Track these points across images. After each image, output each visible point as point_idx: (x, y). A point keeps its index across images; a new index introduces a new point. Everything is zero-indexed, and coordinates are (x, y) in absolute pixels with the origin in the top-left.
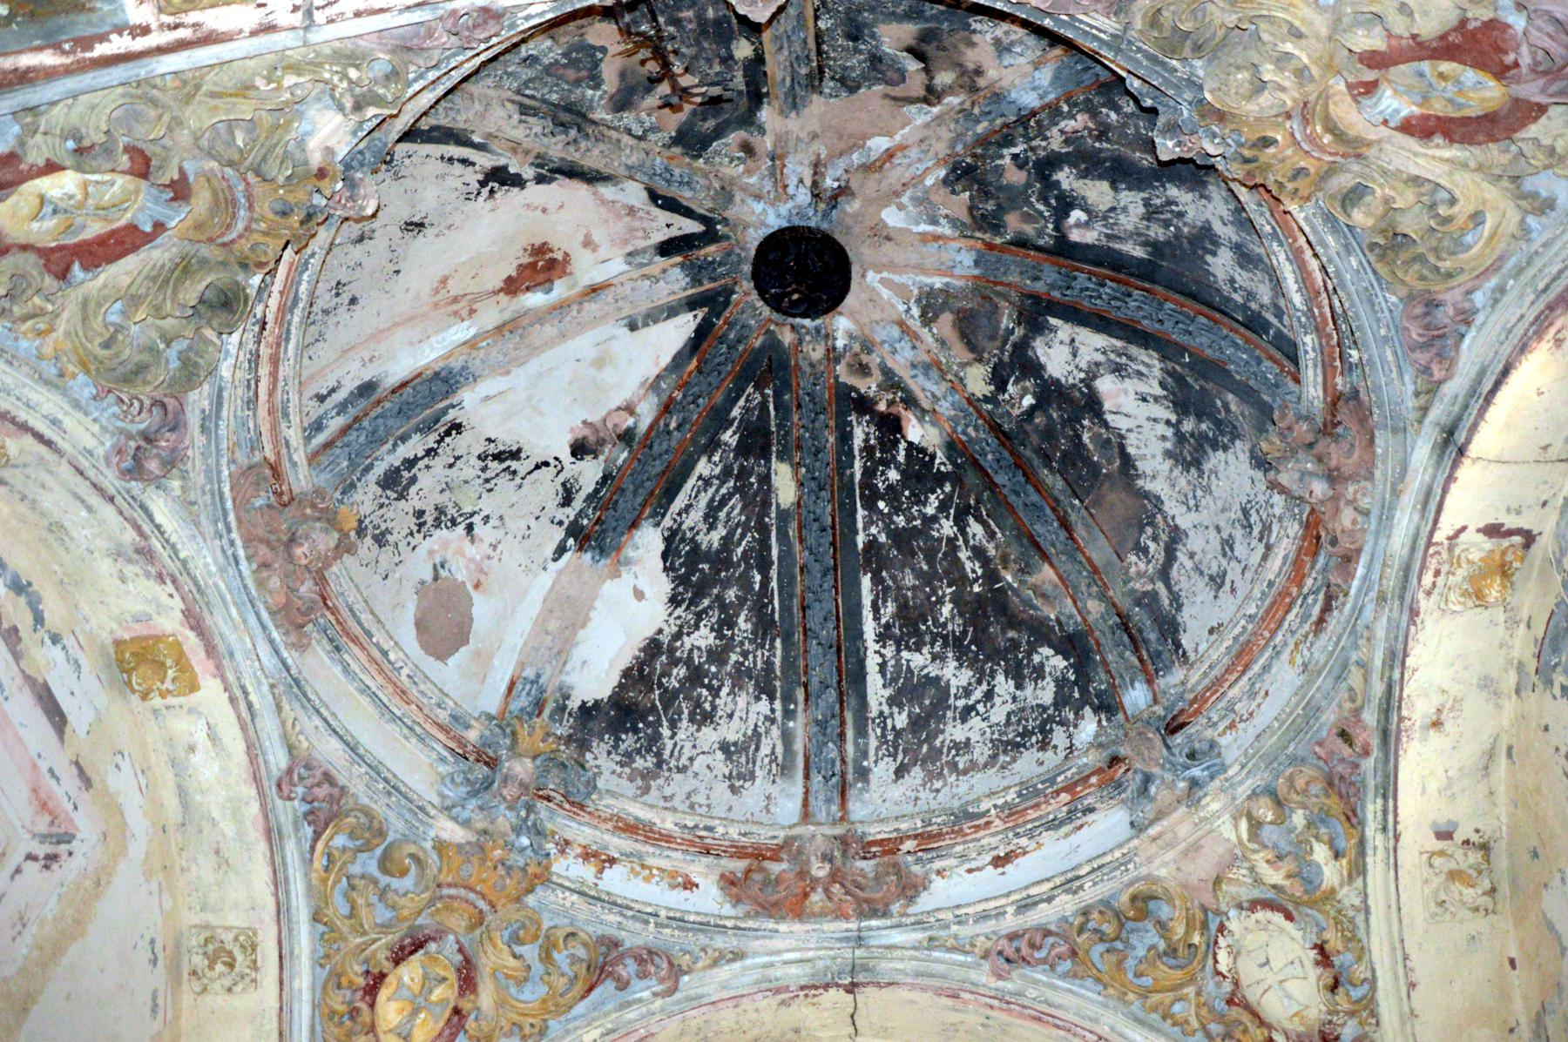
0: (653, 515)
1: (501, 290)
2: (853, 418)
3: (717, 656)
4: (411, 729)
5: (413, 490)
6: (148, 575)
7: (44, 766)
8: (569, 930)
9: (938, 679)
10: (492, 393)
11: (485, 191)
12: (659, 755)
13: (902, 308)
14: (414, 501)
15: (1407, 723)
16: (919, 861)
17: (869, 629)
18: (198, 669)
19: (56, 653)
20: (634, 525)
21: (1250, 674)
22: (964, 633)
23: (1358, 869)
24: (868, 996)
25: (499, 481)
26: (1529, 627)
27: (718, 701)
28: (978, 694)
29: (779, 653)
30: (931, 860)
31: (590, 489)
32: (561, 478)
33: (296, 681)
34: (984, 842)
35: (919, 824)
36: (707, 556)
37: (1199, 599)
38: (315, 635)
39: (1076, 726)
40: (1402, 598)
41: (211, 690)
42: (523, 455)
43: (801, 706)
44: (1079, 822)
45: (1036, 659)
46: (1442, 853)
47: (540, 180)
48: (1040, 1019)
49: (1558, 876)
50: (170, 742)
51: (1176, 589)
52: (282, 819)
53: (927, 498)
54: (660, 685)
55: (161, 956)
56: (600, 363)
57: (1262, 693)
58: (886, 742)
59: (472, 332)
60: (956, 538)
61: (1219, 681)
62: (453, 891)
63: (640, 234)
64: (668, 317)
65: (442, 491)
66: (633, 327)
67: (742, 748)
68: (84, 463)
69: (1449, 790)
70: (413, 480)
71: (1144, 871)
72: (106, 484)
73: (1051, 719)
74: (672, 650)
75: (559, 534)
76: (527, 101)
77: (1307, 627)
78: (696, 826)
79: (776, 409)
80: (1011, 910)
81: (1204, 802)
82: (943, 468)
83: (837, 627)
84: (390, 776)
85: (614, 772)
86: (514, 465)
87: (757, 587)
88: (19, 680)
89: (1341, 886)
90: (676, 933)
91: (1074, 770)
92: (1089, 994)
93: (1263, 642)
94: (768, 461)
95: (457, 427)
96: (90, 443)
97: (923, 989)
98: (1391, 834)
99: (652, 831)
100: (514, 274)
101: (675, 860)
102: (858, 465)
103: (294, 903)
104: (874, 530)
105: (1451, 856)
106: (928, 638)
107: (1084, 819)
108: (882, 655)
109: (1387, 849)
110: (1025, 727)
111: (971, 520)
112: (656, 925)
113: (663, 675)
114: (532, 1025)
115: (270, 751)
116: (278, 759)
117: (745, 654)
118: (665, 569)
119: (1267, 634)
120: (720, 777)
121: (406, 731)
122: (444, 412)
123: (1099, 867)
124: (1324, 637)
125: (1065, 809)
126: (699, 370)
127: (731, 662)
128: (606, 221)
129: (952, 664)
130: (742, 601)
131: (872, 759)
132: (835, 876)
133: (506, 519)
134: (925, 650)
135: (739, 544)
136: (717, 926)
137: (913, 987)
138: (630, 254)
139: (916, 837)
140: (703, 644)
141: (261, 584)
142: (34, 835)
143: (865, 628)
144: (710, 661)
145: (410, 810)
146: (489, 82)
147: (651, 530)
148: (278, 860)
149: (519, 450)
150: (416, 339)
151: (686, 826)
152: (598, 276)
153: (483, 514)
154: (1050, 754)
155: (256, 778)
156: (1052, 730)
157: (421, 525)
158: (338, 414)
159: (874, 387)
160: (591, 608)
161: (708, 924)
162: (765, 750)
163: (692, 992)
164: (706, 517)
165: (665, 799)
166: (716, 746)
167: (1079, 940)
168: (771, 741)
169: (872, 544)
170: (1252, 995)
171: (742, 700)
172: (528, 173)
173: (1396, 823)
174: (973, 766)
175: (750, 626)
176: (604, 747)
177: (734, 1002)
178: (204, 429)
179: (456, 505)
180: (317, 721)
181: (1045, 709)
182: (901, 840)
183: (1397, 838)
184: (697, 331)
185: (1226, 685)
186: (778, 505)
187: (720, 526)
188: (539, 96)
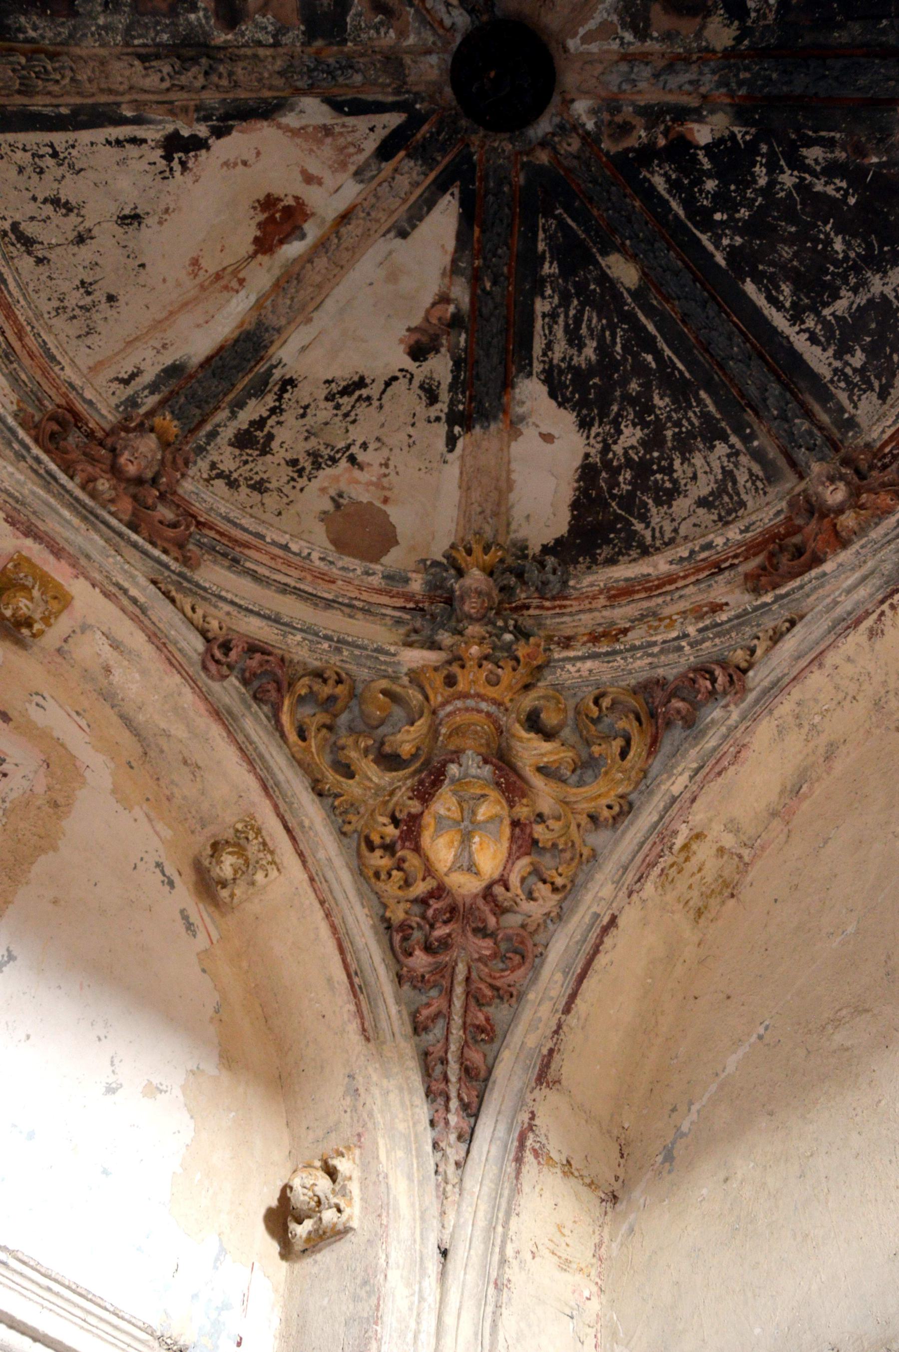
0: (521, 369)
1: (256, 253)
2: (644, 173)
3: (653, 441)
5: (275, 445)
8: (597, 692)
9: (870, 301)
10: (305, 342)
11: (175, 164)
13: (615, 46)
14: (280, 454)
17: (779, 321)
18: (59, 579)
20: (507, 384)
22: (869, 247)
25: (358, 411)
27: (675, 475)
29: (708, 401)
31: (449, 380)
32: (416, 383)
36: (592, 371)
38: (206, 557)
42: (368, 381)
47: (220, 132)
52: (227, 700)
53: (753, 174)
54: (613, 497)
56: (393, 277)
58: (856, 385)
59: (253, 298)
60: (802, 179)
63: (352, 150)
64: (429, 210)
65: (306, 439)
66: (403, 234)
67: (718, 493)
70: (270, 437)
74: (607, 464)
75: (442, 429)
76: (142, 51)
78: (692, 552)
79: (574, 220)
82: (748, 138)
83: (747, 340)
84: (330, 633)
86: (364, 392)
87: (654, 365)
90: (717, 641)
94: (597, 264)
95: (289, 383)
100: (258, 233)
102: (674, 204)
103: (281, 777)
104: (725, 242)
108: (807, 330)
111: (804, 151)
112: (691, 645)
113: (611, 488)
114: (610, 807)
115: (179, 638)
117: (678, 424)
118: (560, 405)
122: (269, 373)
126: (483, 232)
128: (311, 150)
130: (647, 387)
133: (385, 439)
134: (843, 293)
135: (614, 343)
136: (756, 609)
138: (356, 174)
140: (633, 441)
141: (93, 495)
143: (775, 323)
144: (649, 450)
145: (368, 657)
146: (90, 41)
147: (527, 381)
148: (241, 738)
149: (362, 378)
150: (201, 321)
151: (682, 559)
152: (340, 204)
153: (358, 444)
155: (179, 669)
157: (300, 472)
158: (152, 393)
159: (643, 133)
160: (509, 472)
161: (745, 613)
162: (742, 478)
163: (766, 683)
164: (570, 342)
169: (732, 254)
171: (698, 460)
172: (202, 130)
175: (667, 400)
177: (816, 663)
179: (327, 445)
180: (227, 608)
184: (462, 204)
186: (628, 290)
187: (587, 342)
188: (150, 42)
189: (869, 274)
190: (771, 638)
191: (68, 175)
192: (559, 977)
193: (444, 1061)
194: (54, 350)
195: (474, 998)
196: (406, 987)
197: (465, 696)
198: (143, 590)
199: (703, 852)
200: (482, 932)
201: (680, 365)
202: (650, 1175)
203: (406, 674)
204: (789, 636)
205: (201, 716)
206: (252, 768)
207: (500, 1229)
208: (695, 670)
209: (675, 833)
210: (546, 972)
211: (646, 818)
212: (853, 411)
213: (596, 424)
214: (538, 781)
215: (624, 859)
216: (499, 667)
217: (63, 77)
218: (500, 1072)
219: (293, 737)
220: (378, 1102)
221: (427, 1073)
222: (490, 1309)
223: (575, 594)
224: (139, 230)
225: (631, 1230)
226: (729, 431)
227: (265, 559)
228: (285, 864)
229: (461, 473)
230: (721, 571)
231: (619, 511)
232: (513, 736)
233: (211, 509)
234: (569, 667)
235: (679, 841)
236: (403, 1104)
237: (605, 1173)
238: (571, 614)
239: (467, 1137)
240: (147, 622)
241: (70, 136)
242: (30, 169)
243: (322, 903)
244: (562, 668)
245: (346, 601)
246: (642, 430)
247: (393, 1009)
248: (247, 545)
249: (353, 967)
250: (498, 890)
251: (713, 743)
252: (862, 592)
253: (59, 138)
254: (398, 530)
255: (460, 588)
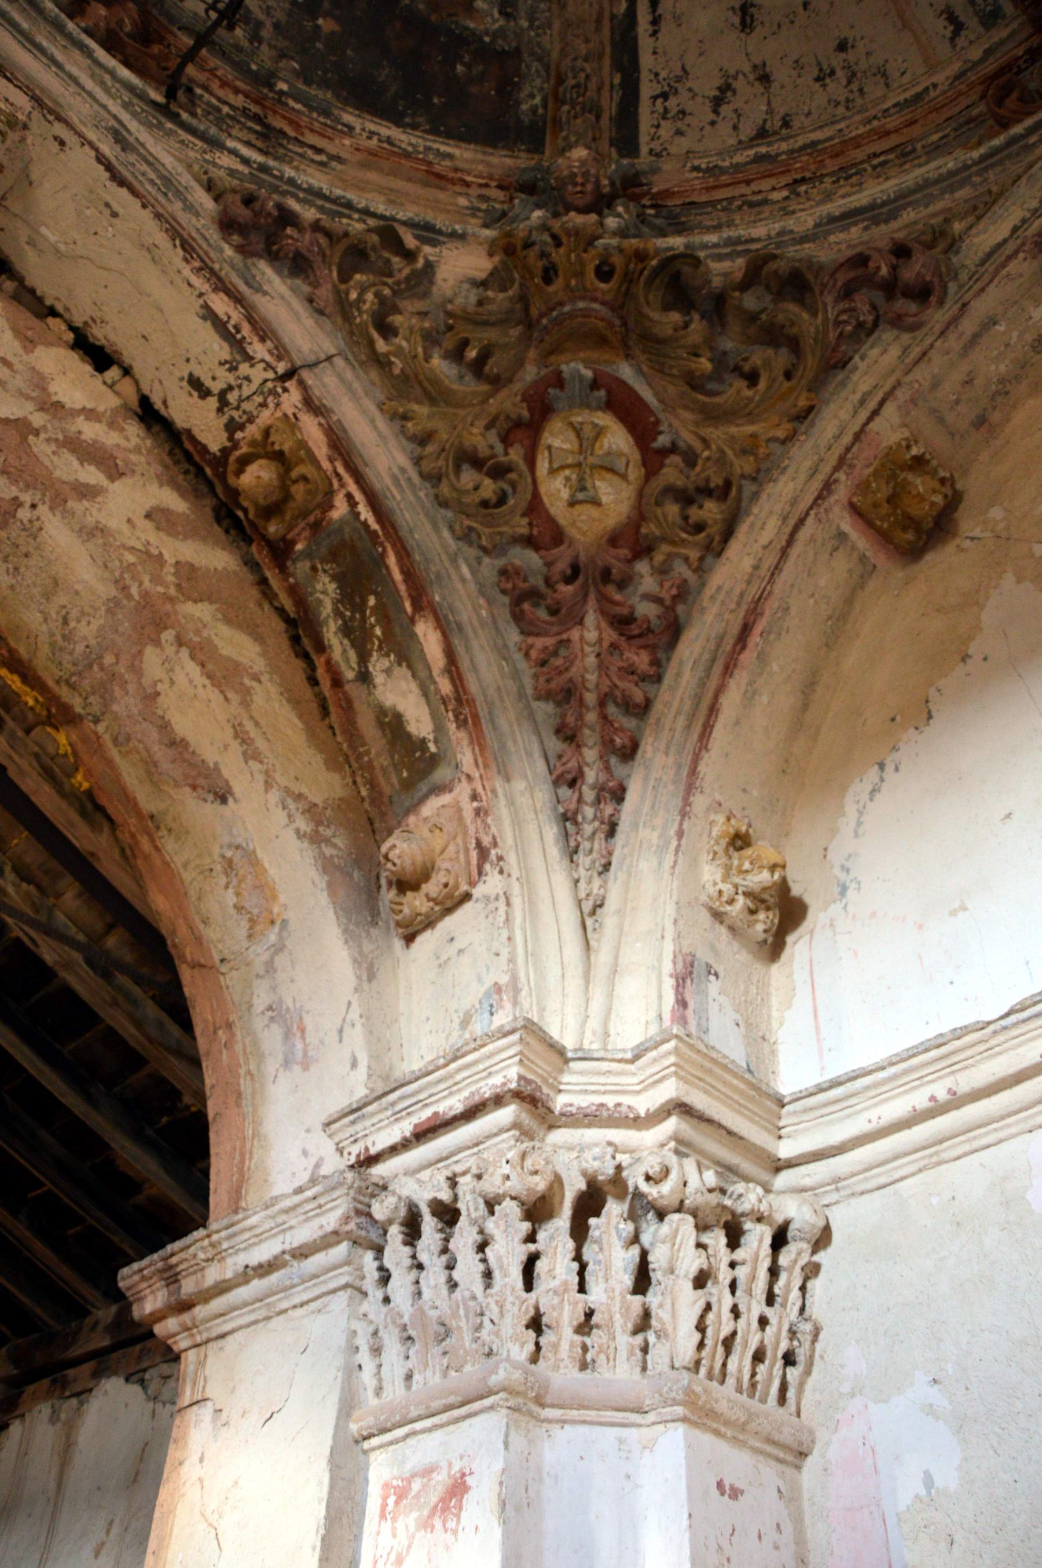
68: (916, 352)
72: (947, 317)
96: (895, 352)
178: (893, 215)
191: (689, 85)
194: (907, 95)
217: (583, 70)
224: (760, 7)
241: (645, 76)
242: (679, 124)
253: (647, 89)
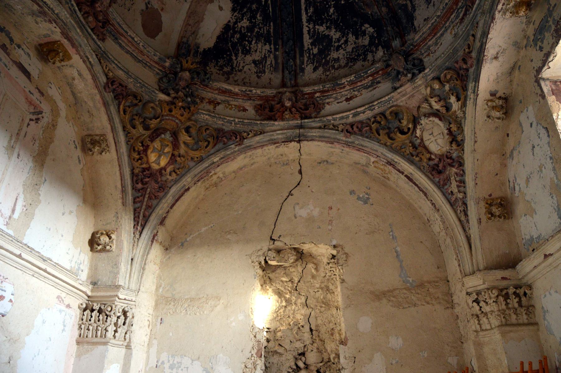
3: (250, 29)
4: (146, 64)
6: (45, 21)
7: (27, 90)
8: (206, 127)
9: (329, 35)
12: (232, 66)
15: (486, 57)
16: (321, 99)
17: (304, 18)
19: (20, 51)
21: (436, 37)
22: (338, 19)
23: (464, 105)
24: (304, 144)
26: (534, 24)
27: (251, 46)
28: (342, 41)
29: (272, 27)
30: (325, 99)
33: (104, 52)
34: (343, 93)
35: (321, 87)
37: (421, 8)
39: (376, 53)
40: (490, 13)
41: (76, 59)
43: (280, 47)
44: (375, 87)
45: (363, 28)
46: (491, 101)
48: (359, 150)
49: (526, 109)
50: (65, 77)
51: (414, 3)
52: (108, 99)
54: (231, 41)
55: (78, 146)
57: (440, 44)
58: (310, 59)
61: (425, 39)
62: (167, 118)
69: (497, 80)
71: (395, 103)
73: (367, 50)
74: (234, 28)
77: (458, 20)
78: (246, 90)
80: (351, 116)
81: (416, 81)
84: (141, 82)
85: (217, 73)
88: (11, 63)
89: (458, 110)
90: (241, 126)
91: (374, 69)
92: (375, 143)
93: (441, 25)
97: (322, 141)
98: (476, 94)
99: (231, 93)
101: (240, 102)
103: (116, 125)
105: (494, 101)
106: (325, 21)
107: (377, 86)
108: (309, 27)
109: (474, 99)
110: (358, 53)
113: (231, 38)
114: (197, 158)
116: (103, 79)
117: (260, 28)
119: (443, 23)
120: (253, 73)
121: (144, 65)
123: (380, 102)
124: (463, 24)
125: (370, 82)
127: (255, 31)
129: (334, 30)
131: (306, 65)
132: (293, 106)
134: (324, 25)
137: (319, 141)
139: (320, 92)
140: (245, 25)
142: (30, 113)
144: (248, 32)
148: (109, 113)
151: (242, 91)
154: (366, 63)
155: (97, 87)
156: (367, 54)
160: (204, 15)
162: (268, 63)
163: (248, 144)
165: (235, 81)
166: (251, 62)
167: (373, 126)
168: (270, 60)
170: (427, 143)
171: (260, 45)
173: (478, 90)
174: (340, 67)
175: (261, 18)
176: (213, 64)
180: (114, 66)
181: (365, 46)
182: (315, 93)
183: (477, 95)
185: (428, 40)
189: (333, 27)
190: (254, 134)
192: (171, 198)
193: (139, 213)
195: (150, 198)
196: (134, 190)
197: (173, 116)
198: (94, 59)
199: (215, 177)
200: (157, 182)
201: (270, 9)
202: (177, 247)
203: (158, 101)
204: (258, 136)
205: (100, 104)
206: (110, 124)
207: (145, 256)
208: (233, 133)
209: (211, 172)
210: (168, 196)
211: (205, 164)
212: (306, 67)
213: (237, 12)
214: (182, 146)
215: (196, 173)
216: (185, 111)
218: (152, 218)
219: (122, 113)
220: (124, 221)
221: (134, 214)
222: (141, 274)
223: (210, 86)
225: (169, 258)
226: (272, 43)
227: (126, 41)
228: (112, 151)
229: (189, 8)
230: (250, 99)
231: (230, 48)
232: (181, 132)
233: (115, 19)
234: (202, 115)
235: (211, 174)
236: (128, 222)
237: (167, 244)
238: (206, 91)
239: (141, 233)
240: (92, 71)
243: (119, 166)
244: (200, 115)
245: (145, 62)
246: (249, 23)
247: (130, 198)
248: (122, 35)
249: (123, 185)
250: (163, 171)
251: (229, 153)
252: (280, 136)
254: (163, 24)
255: (181, 75)
